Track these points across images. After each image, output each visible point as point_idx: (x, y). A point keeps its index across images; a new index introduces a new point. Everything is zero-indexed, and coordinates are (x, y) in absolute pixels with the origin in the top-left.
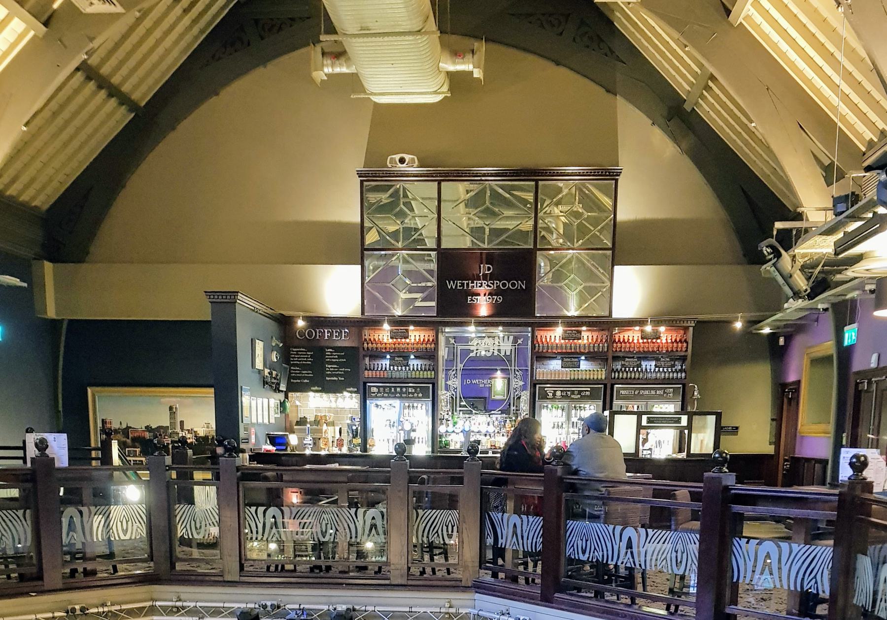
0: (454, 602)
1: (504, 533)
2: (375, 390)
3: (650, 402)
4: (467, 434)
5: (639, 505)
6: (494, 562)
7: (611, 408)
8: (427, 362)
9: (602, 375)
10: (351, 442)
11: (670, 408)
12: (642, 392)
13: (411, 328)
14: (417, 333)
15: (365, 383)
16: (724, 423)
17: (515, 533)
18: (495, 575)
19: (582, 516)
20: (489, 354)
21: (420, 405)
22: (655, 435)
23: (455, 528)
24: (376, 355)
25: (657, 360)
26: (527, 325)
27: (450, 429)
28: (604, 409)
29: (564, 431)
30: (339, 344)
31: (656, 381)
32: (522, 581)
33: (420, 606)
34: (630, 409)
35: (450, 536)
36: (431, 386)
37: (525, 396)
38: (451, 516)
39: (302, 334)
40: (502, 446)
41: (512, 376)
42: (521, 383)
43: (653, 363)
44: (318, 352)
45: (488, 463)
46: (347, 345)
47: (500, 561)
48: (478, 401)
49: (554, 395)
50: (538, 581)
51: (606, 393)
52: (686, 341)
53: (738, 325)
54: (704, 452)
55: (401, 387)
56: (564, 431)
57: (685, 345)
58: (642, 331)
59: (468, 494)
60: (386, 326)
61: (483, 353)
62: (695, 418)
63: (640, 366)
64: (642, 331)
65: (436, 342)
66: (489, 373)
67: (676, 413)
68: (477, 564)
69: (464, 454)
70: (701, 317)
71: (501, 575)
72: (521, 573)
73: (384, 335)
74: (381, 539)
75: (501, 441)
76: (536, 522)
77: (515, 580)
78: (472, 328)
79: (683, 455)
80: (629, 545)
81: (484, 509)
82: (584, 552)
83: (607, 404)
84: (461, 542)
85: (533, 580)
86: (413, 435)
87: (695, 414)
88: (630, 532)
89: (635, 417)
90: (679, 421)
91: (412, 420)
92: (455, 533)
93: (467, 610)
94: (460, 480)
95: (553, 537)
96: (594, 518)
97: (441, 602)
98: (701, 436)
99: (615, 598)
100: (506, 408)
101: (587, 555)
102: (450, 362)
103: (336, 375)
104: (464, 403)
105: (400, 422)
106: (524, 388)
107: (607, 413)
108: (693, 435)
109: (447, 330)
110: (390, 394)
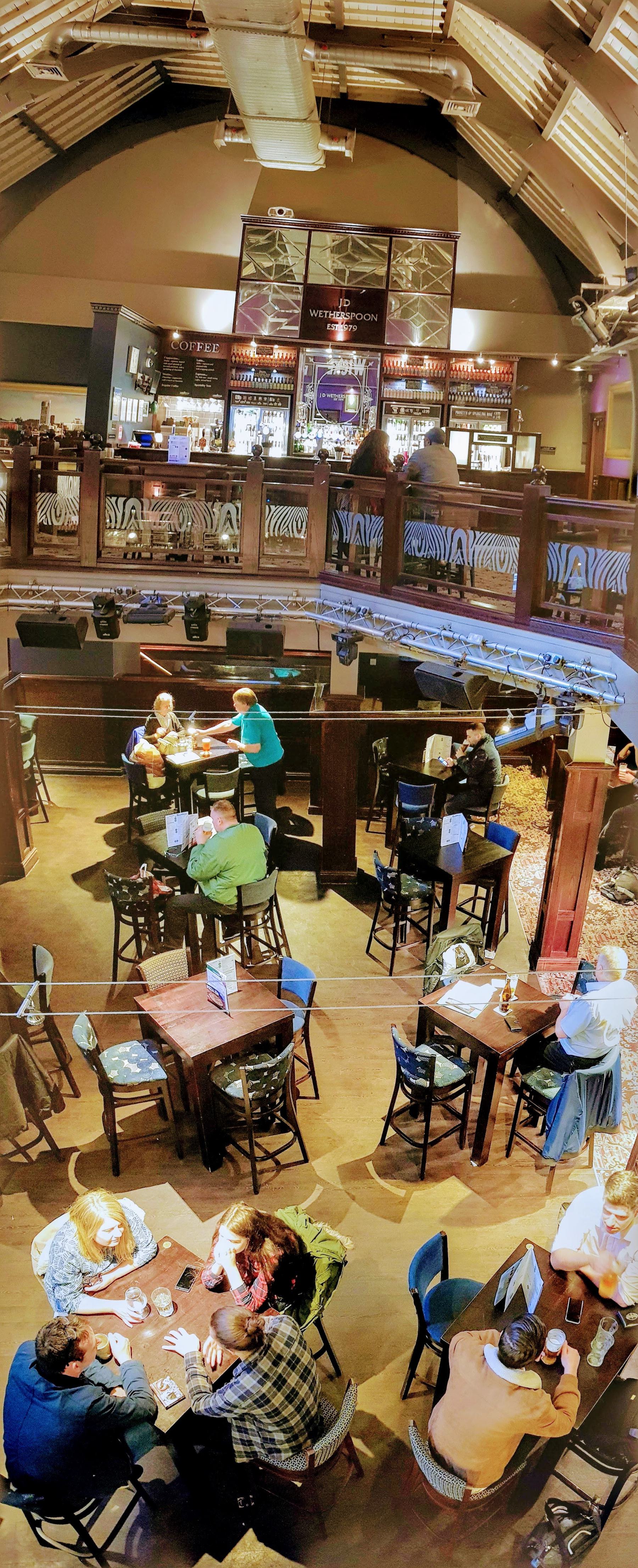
0: (301, 592)
1: (349, 529)
2: (239, 397)
3: (480, 421)
4: (319, 440)
5: (469, 510)
6: (339, 556)
7: (448, 425)
8: (288, 377)
9: (440, 396)
10: (213, 442)
11: (497, 428)
12: (474, 413)
13: (276, 346)
14: (281, 352)
15: (230, 391)
16: (542, 445)
17: (359, 530)
18: (339, 568)
19: (421, 518)
20: (344, 374)
21: (279, 413)
22: (485, 450)
23: (304, 524)
24: (243, 367)
25: (487, 387)
26: (377, 350)
27: (305, 435)
28: (442, 425)
29: (406, 443)
30: (209, 356)
31: (486, 405)
32: (363, 573)
33: (270, 595)
34: (464, 427)
35: (299, 532)
36: (289, 397)
37: (373, 410)
38: (301, 512)
39: (176, 345)
40: (352, 453)
41: (362, 392)
42: (371, 399)
43: (484, 390)
44: (189, 360)
45: (339, 466)
46: (217, 357)
47: (344, 557)
48: (332, 412)
49: (399, 410)
50: (378, 574)
51: (443, 412)
52: (511, 373)
53: (555, 363)
54: (526, 467)
55: (263, 397)
56: (406, 443)
57: (511, 376)
58: (475, 363)
59: (317, 492)
60: (253, 344)
61: (338, 372)
62: (520, 439)
63: (473, 391)
64: (475, 363)
65: (297, 359)
66: (342, 390)
67: (502, 433)
68: (324, 557)
69: (316, 458)
70: (524, 354)
71: (345, 568)
72: (363, 567)
73: (251, 351)
74: (237, 532)
75: (351, 449)
76: (378, 522)
77: (357, 572)
78: (329, 351)
79: (509, 469)
80: (460, 546)
81: (332, 509)
82: (419, 551)
83: (445, 422)
84: (309, 537)
85: (374, 574)
86: (271, 439)
87: (519, 434)
88: (460, 533)
89: (468, 434)
90: (505, 439)
91: (271, 426)
92: (304, 529)
93: (313, 600)
94: (311, 481)
95: (393, 538)
96: (430, 519)
97: (290, 591)
98: (524, 453)
99: (446, 592)
100: (357, 420)
101: (422, 553)
102: (308, 378)
103: (204, 383)
104: (319, 414)
105: (259, 427)
106: (372, 404)
107: (444, 429)
108: (517, 453)
109: (308, 350)
110: (253, 402)
